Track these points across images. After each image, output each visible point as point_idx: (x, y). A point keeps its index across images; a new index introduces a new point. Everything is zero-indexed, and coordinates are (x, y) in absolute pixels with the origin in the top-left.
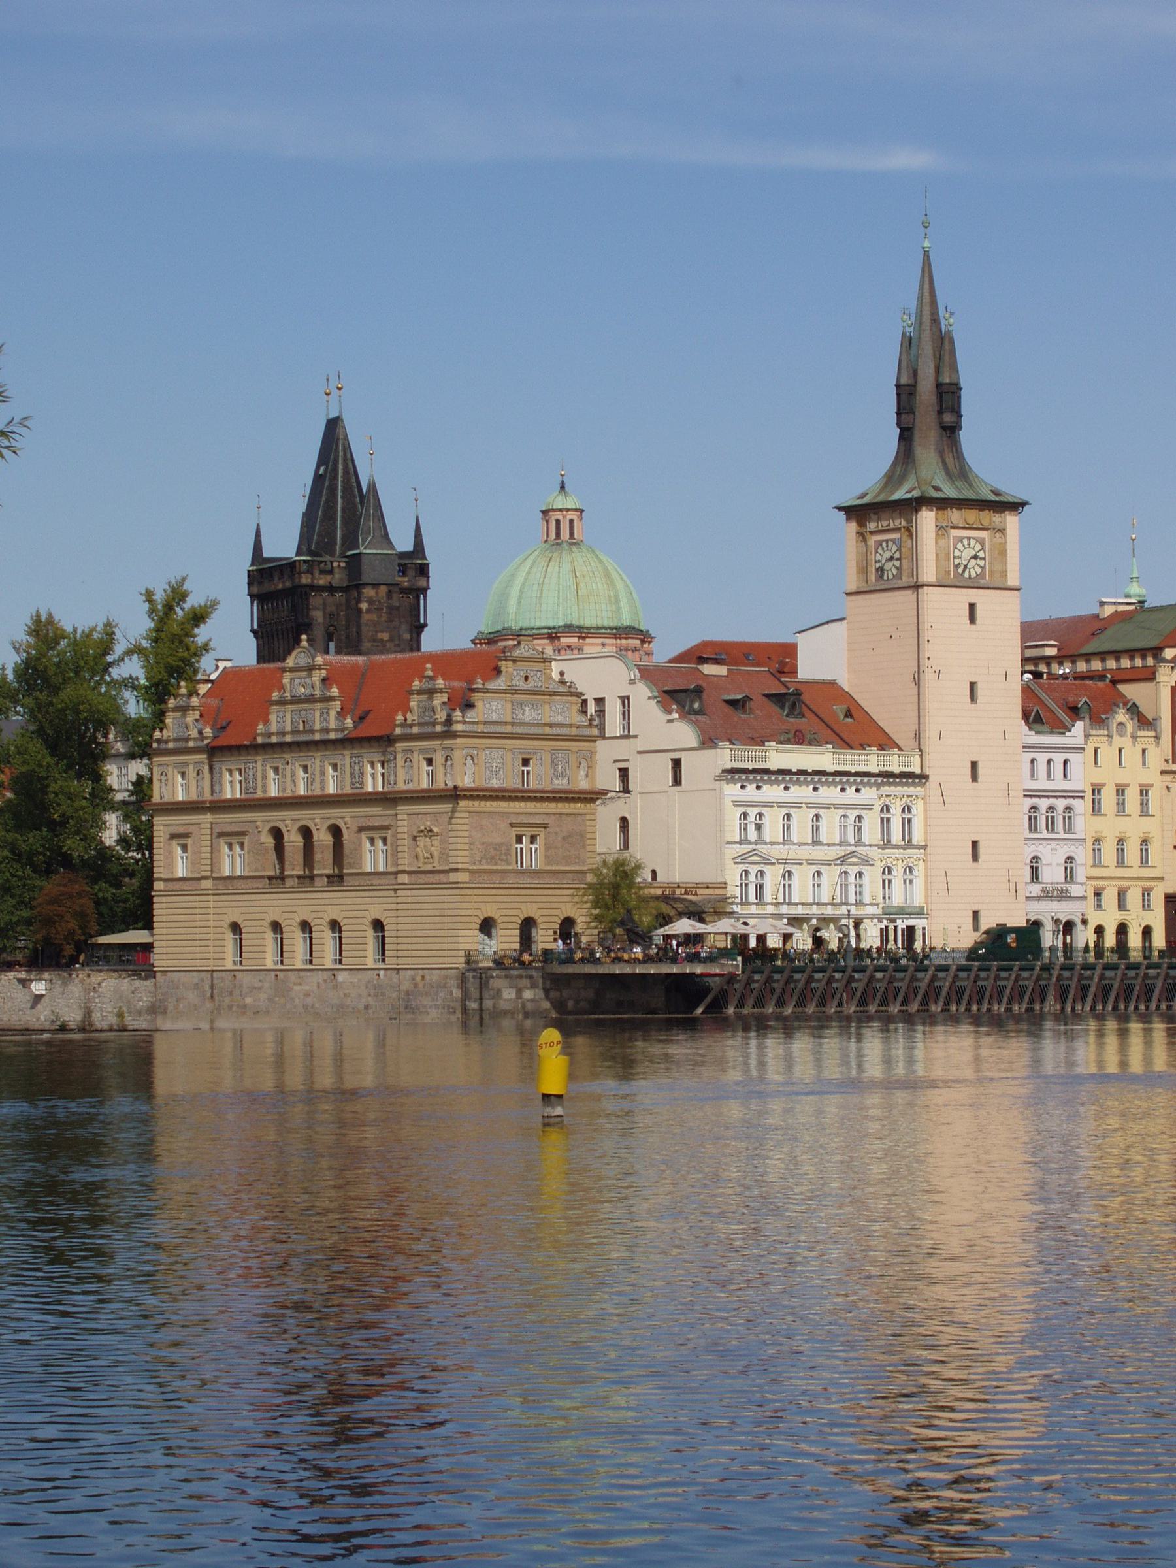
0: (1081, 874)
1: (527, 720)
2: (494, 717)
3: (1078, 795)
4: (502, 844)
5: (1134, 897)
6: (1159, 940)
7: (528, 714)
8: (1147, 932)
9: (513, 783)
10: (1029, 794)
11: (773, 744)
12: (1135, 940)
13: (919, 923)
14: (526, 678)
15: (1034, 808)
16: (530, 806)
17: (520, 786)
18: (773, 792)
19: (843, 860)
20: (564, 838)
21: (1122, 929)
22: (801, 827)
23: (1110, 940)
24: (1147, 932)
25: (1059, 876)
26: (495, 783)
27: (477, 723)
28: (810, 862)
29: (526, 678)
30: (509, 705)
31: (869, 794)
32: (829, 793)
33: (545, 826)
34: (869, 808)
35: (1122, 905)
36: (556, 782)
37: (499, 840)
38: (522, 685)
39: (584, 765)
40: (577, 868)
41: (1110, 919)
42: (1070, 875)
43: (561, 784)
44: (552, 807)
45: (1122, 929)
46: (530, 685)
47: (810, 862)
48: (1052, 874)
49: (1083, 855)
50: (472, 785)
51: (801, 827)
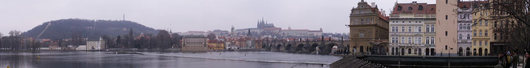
0: (471, 38)
3: (471, 22)
5: (483, 42)
6: (489, 52)
7: (362, 12)
8: (486, 50)
9: (360, 24)
10: (459, 22)
12: (483, 52)
13: (435, 48)
15: (461, 25)
16: (362, 28)
18: (400, 23)
19: (415, 36)
21: (480, 50)
22: (407, 29)
23: (477, 52)
24: (486, 50)
25: (466, 38)
28: (408, 36)
31: (423, 23)
32: (413, 23)
34: (422, 25)
35: (480, 44)
41: (477, 47)
42: (468, 38)
44: (366, 27)
45: (480, 50)
47: (408, 36)
48: (465, 38)
49: (471, 34)
51: (407, 29)
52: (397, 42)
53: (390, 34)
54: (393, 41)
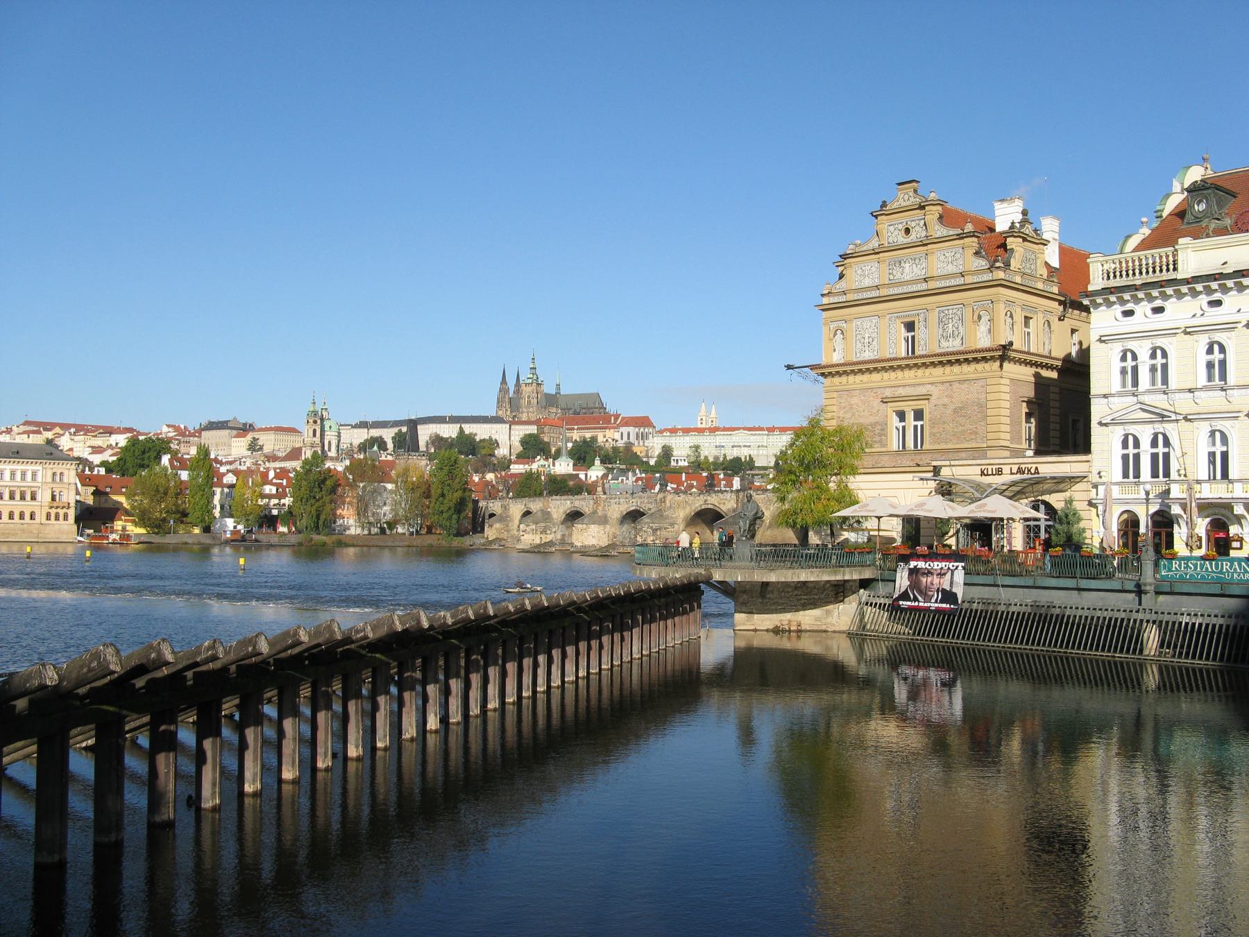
1: (908, 278)
2: (867, 282)
4: (876, 423)
11: (1187, 240)
14: (907, 231)
17: (903, 354)
20: (955, 411)
26: (867, 355)
27: (844, 293)
29: (907, 231)
30: (884, 267)
33: (927, 397)
36: (944, 344)
37: (872, 419)
38: (905, 241)
39: (985, 318)
40: (974, 445)
43: (954, 345)
46: (913, 237)
50: (842, 361)
52: (1161, 466)
53: (1098, 409)
54: (1130, 466)
